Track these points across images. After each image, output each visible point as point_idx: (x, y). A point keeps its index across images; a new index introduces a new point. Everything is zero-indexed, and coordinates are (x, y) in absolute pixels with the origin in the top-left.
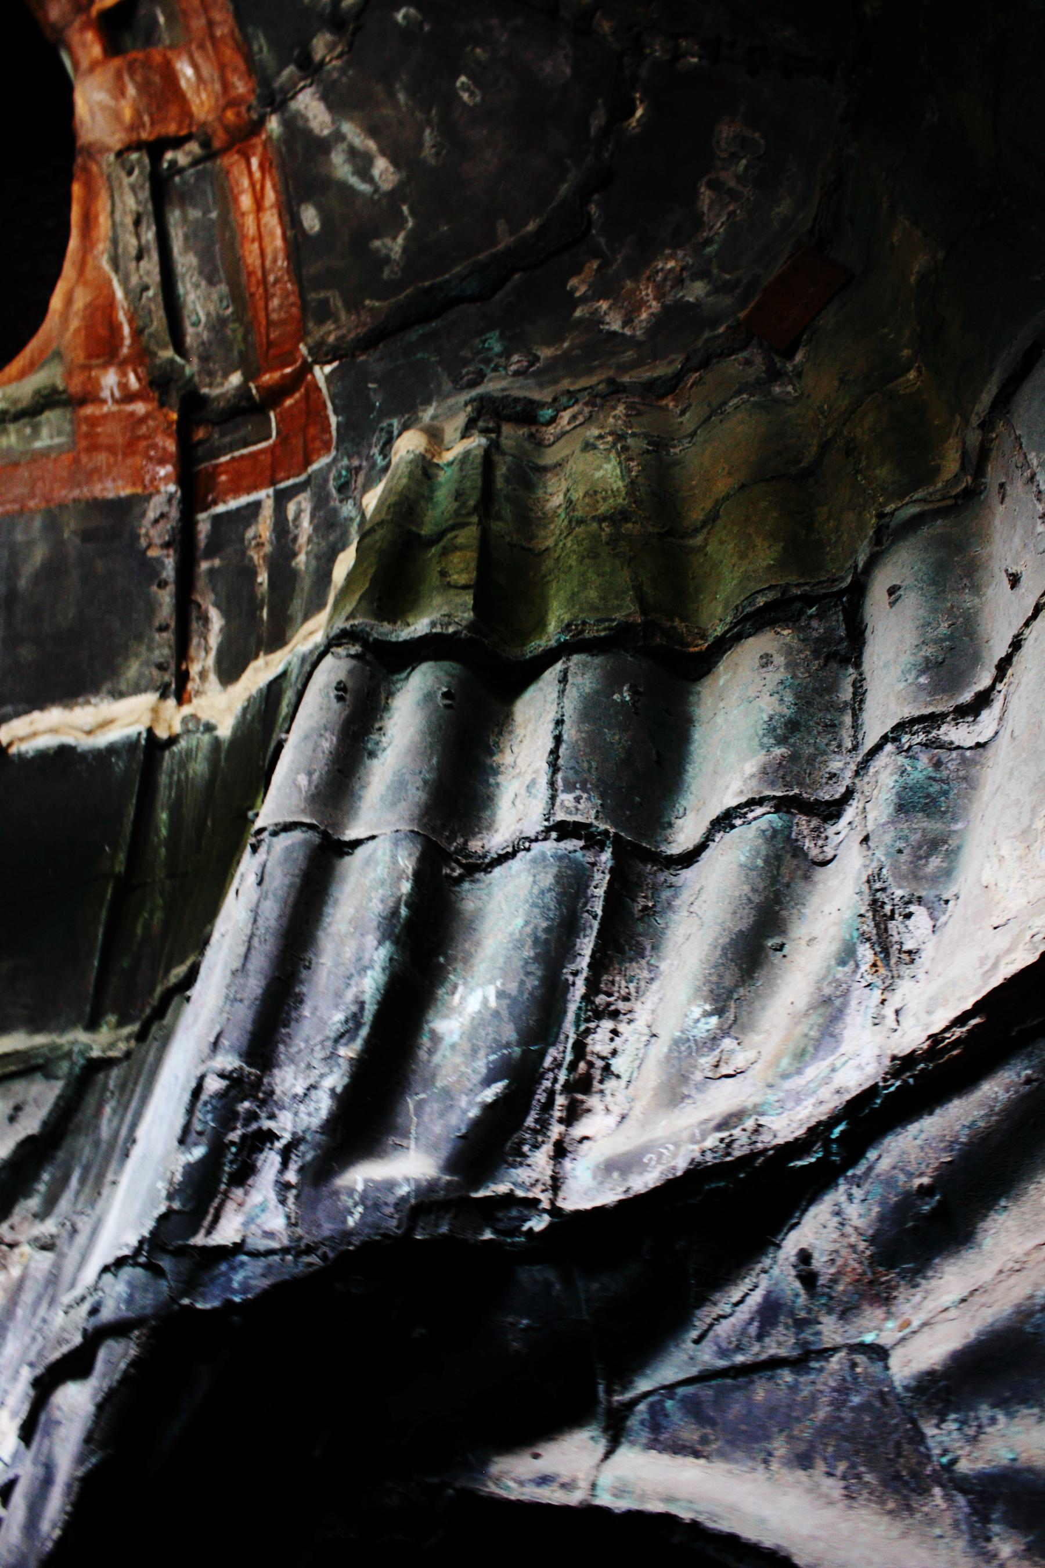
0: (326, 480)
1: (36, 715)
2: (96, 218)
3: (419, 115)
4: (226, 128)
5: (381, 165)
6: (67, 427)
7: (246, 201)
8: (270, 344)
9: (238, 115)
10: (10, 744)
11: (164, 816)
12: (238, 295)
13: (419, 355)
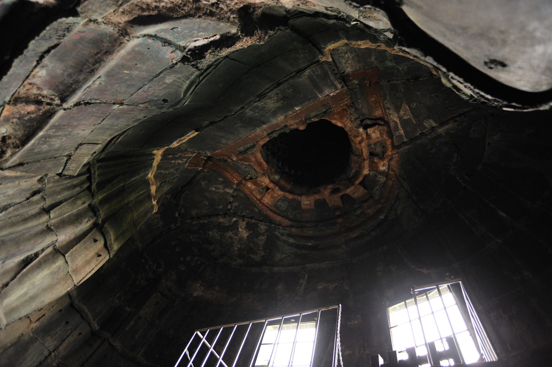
5: (214, 189)
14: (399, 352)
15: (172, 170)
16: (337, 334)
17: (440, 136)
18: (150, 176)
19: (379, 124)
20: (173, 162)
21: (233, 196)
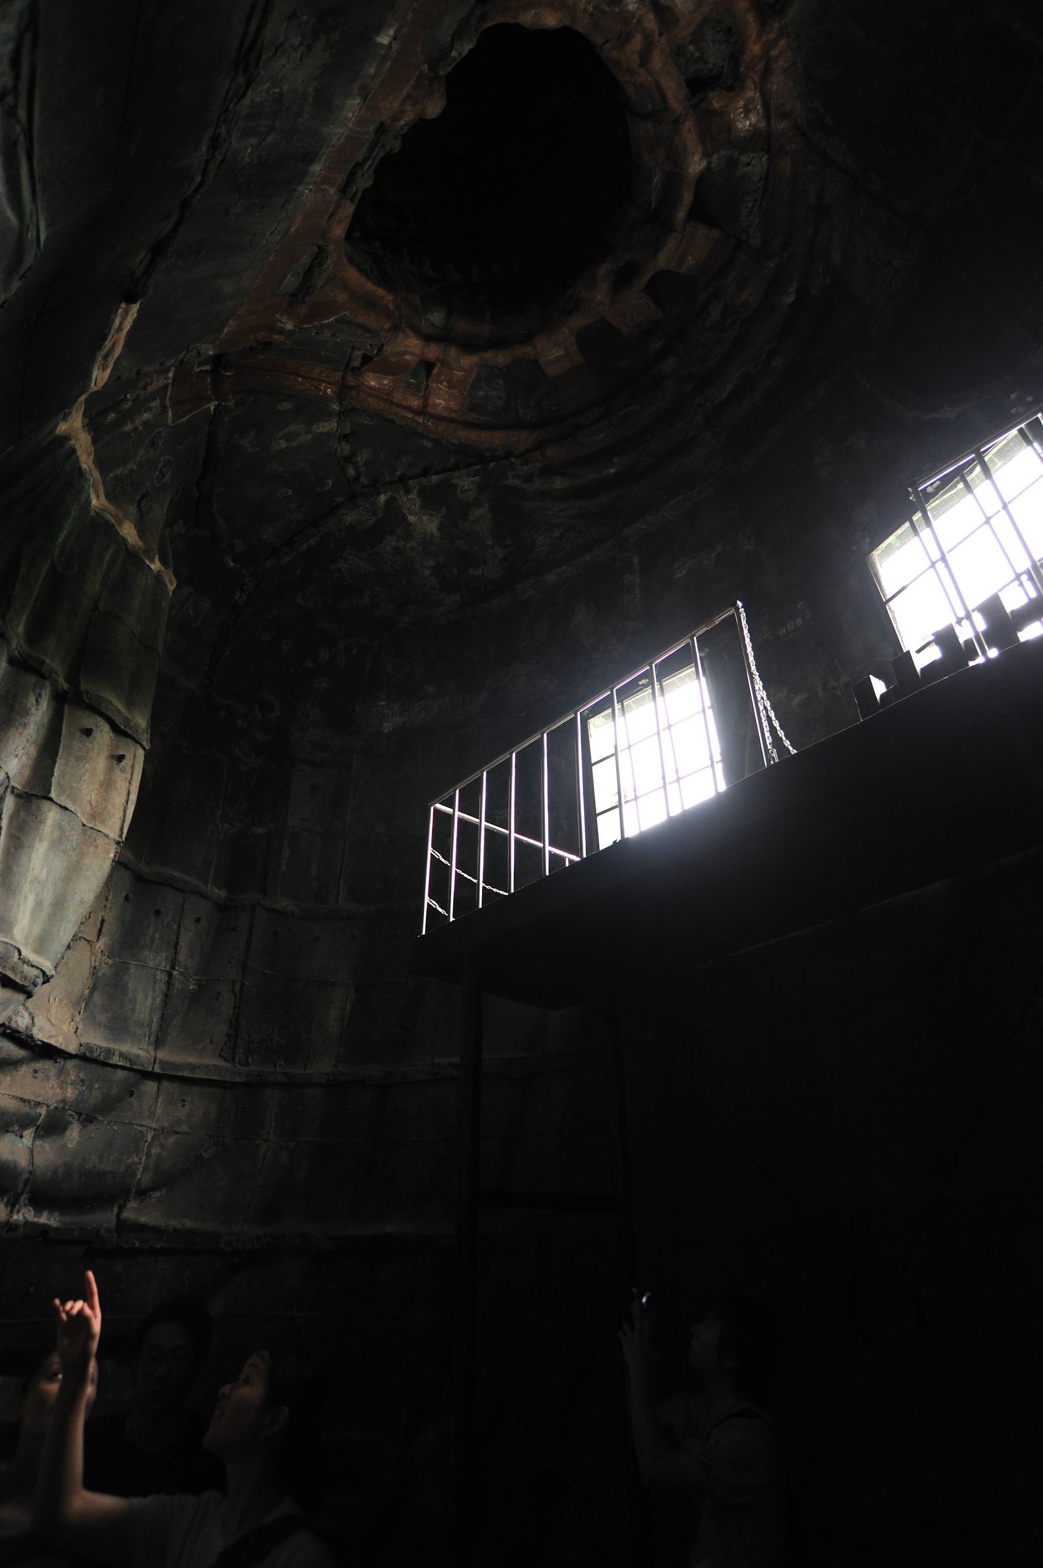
5: (283, 445)
14: (918, 651)
15: (142, 452)
16: (751, 674)
18: (97, 501)
20: (129, 427)
21: (345, 437)
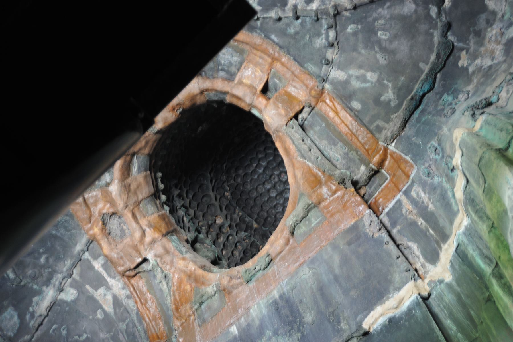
0: (420, 177)
1: (372, 313)
2: (289, 147)
3: (372, 52)
4: (314, 97)
6: (320, 214)
7: (332, 114)
8: (367, 151)
9: (315, 90)
10: (369, 329)
11: (449, 322)
12: (346, 143)
13: (423, 119)
17: (48, 282)
19: (130, 270)
21: (328, 63)
